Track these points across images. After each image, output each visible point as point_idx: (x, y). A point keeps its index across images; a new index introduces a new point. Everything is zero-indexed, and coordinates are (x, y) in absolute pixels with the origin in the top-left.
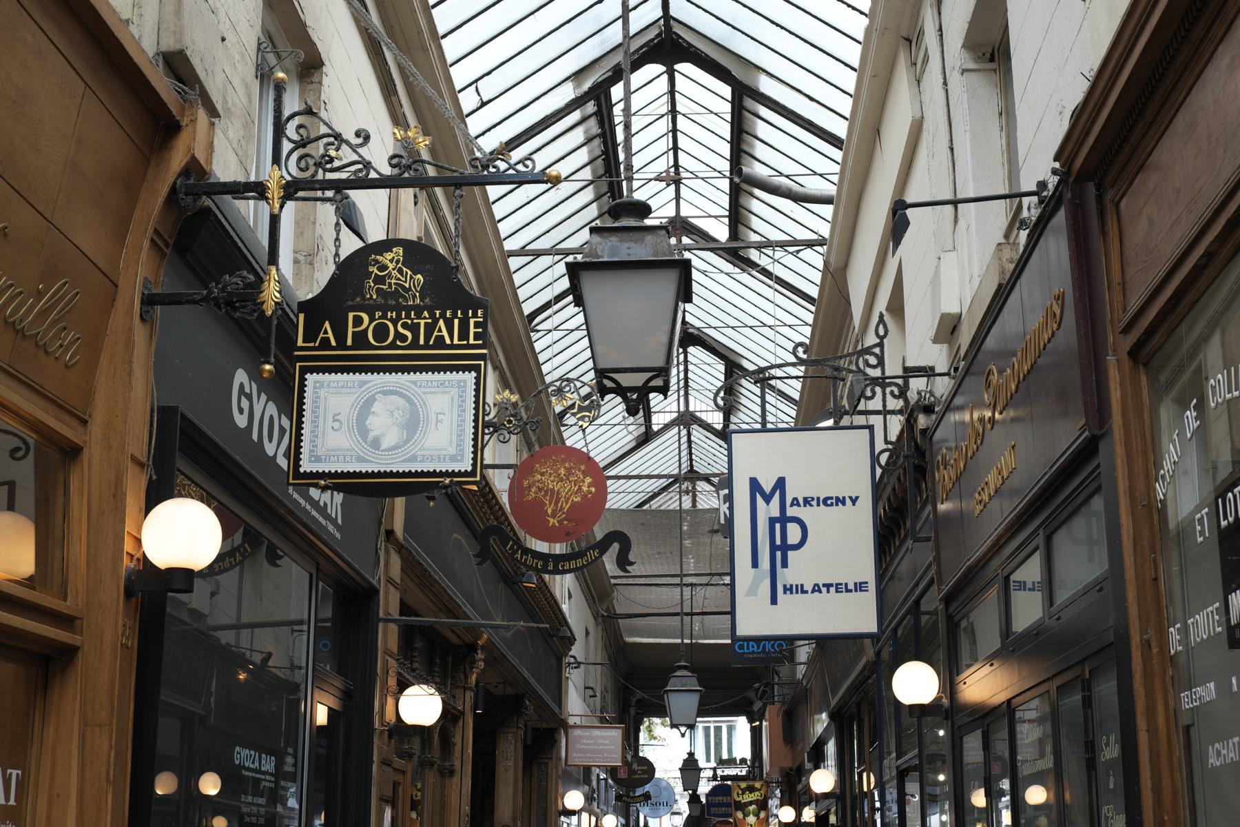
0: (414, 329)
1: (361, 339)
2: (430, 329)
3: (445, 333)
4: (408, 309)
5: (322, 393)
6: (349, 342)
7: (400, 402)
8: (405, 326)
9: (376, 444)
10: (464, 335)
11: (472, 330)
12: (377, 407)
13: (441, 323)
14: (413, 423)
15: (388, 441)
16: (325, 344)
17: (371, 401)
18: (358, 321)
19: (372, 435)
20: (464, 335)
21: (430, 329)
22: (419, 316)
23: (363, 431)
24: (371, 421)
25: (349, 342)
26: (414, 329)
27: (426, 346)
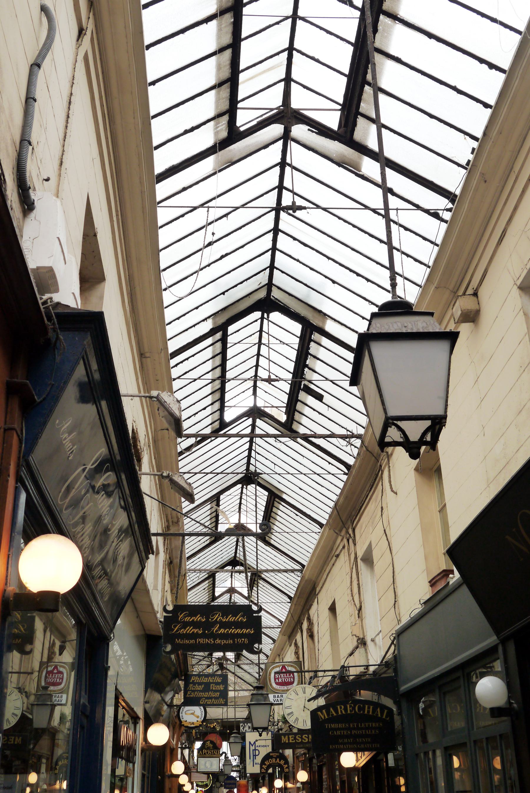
0: (211, 752)
1: (205, 754)
2: (213, 752)
10: (217, 753)
16: (200, 754)
20: (217, 753)
21: (213, 752)
26: (211, 752)
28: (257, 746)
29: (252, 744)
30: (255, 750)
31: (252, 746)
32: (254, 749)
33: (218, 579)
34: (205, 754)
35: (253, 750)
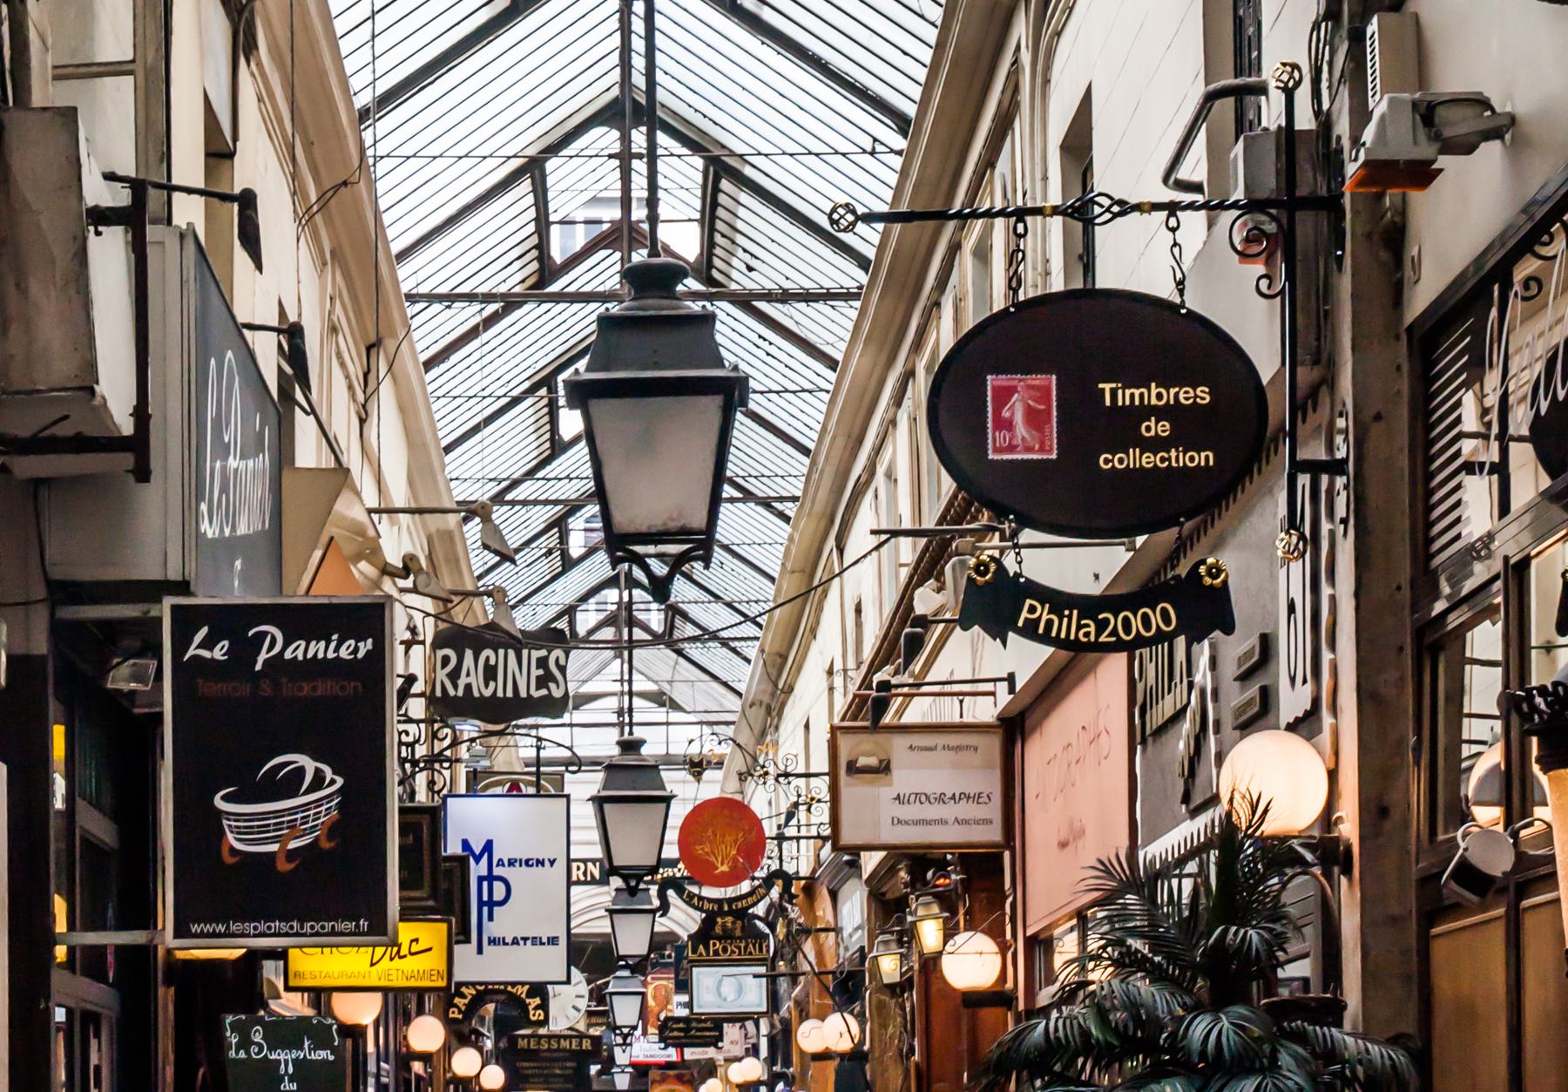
0: (739, 948)
2: (746, 948)
5: (701, 976)
6: (711, 953)
8: (735, 947)
9: (725, 1000)
13: (751, 945)
14: (740, 990)
15: (731, 997)
16: (701, 955)
18: (714, 945)
19: (723, 996)
21: (746, 948)
22: (741, 942)
24: (722, 989)
25: (711, 953)
26: (739, 948)
28: (501, 863)
29: (477, 852)
30: (491, 878)
31: (478, 859)
32: (485, 873)
33: (562, 186)
34: (716, 953)
35: (481, 879)
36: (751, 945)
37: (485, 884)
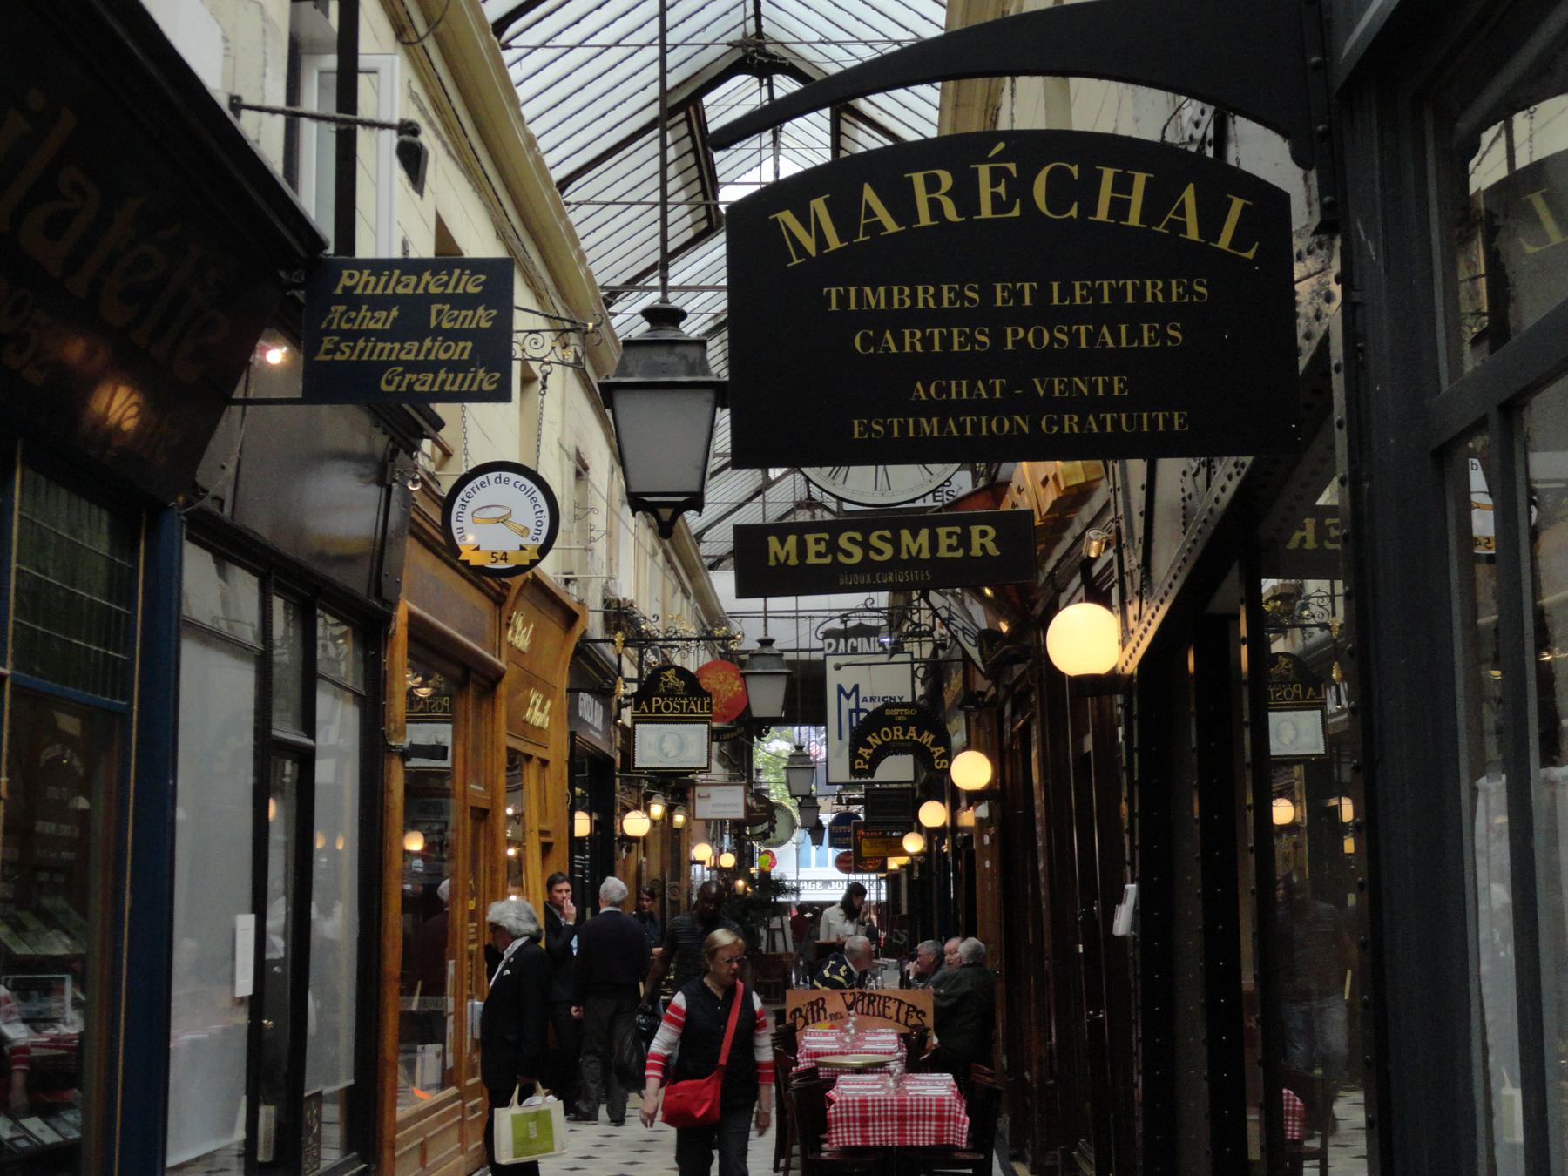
0: (681, 705)
1: (658, 710)
2: (688, 705)
3: (694, 707)
4: (678, 696)
7: (675, 736)
9: (667, 755)
10: (702, 708)
11: (706, 706)
12: (666, 739)
13: (692, 703)
17: (664, 736)
18: (657, 701)
19: (665, 751)
20: (702, 708)
21: (688, 705)
23: (661, 749)
24: (664, 745)
26: (681, 705)
27: (686, 713)
31: (848, 697)
34: (658, 710)
35: (851, 711)
36: (692, 703)
37: (854, 714)
